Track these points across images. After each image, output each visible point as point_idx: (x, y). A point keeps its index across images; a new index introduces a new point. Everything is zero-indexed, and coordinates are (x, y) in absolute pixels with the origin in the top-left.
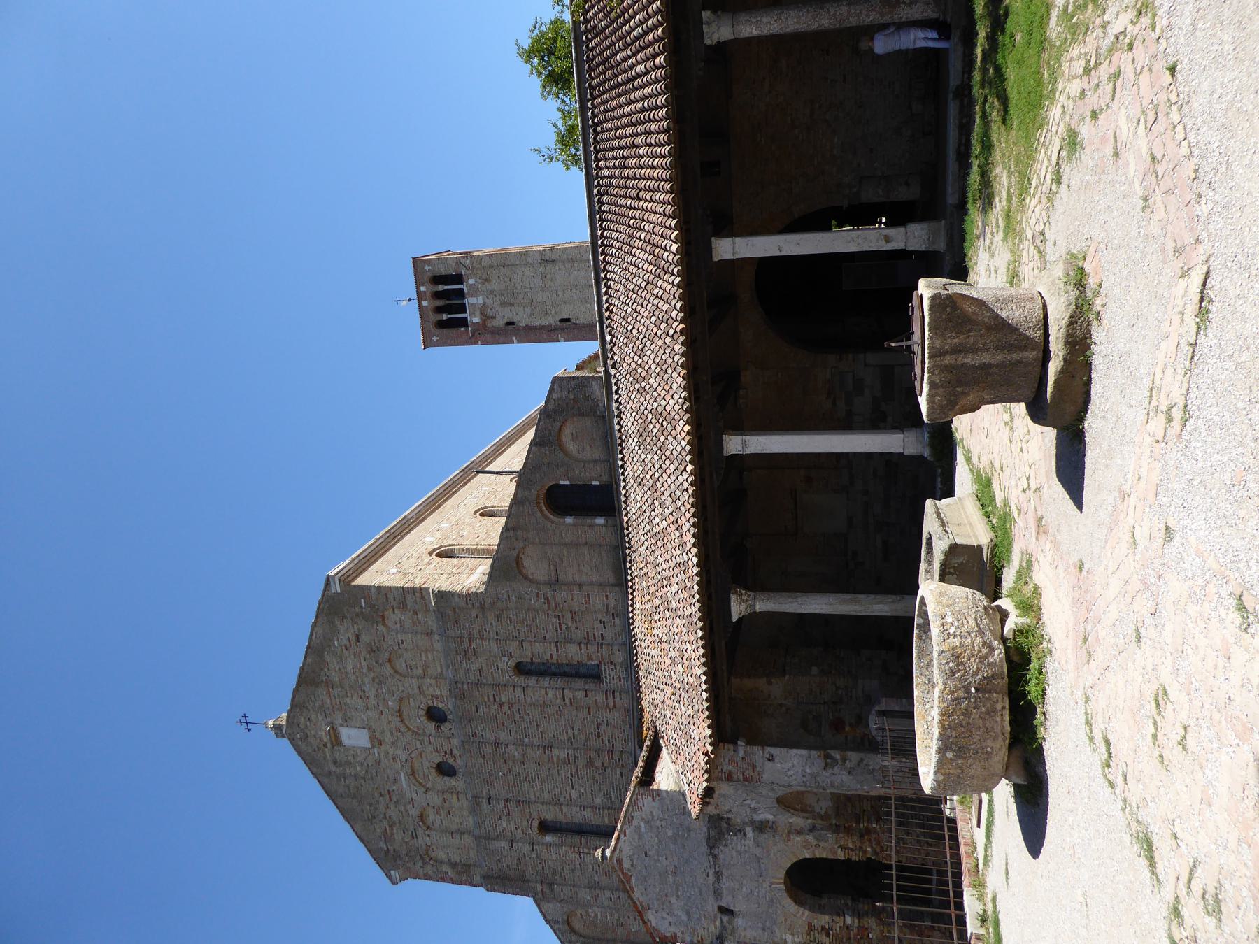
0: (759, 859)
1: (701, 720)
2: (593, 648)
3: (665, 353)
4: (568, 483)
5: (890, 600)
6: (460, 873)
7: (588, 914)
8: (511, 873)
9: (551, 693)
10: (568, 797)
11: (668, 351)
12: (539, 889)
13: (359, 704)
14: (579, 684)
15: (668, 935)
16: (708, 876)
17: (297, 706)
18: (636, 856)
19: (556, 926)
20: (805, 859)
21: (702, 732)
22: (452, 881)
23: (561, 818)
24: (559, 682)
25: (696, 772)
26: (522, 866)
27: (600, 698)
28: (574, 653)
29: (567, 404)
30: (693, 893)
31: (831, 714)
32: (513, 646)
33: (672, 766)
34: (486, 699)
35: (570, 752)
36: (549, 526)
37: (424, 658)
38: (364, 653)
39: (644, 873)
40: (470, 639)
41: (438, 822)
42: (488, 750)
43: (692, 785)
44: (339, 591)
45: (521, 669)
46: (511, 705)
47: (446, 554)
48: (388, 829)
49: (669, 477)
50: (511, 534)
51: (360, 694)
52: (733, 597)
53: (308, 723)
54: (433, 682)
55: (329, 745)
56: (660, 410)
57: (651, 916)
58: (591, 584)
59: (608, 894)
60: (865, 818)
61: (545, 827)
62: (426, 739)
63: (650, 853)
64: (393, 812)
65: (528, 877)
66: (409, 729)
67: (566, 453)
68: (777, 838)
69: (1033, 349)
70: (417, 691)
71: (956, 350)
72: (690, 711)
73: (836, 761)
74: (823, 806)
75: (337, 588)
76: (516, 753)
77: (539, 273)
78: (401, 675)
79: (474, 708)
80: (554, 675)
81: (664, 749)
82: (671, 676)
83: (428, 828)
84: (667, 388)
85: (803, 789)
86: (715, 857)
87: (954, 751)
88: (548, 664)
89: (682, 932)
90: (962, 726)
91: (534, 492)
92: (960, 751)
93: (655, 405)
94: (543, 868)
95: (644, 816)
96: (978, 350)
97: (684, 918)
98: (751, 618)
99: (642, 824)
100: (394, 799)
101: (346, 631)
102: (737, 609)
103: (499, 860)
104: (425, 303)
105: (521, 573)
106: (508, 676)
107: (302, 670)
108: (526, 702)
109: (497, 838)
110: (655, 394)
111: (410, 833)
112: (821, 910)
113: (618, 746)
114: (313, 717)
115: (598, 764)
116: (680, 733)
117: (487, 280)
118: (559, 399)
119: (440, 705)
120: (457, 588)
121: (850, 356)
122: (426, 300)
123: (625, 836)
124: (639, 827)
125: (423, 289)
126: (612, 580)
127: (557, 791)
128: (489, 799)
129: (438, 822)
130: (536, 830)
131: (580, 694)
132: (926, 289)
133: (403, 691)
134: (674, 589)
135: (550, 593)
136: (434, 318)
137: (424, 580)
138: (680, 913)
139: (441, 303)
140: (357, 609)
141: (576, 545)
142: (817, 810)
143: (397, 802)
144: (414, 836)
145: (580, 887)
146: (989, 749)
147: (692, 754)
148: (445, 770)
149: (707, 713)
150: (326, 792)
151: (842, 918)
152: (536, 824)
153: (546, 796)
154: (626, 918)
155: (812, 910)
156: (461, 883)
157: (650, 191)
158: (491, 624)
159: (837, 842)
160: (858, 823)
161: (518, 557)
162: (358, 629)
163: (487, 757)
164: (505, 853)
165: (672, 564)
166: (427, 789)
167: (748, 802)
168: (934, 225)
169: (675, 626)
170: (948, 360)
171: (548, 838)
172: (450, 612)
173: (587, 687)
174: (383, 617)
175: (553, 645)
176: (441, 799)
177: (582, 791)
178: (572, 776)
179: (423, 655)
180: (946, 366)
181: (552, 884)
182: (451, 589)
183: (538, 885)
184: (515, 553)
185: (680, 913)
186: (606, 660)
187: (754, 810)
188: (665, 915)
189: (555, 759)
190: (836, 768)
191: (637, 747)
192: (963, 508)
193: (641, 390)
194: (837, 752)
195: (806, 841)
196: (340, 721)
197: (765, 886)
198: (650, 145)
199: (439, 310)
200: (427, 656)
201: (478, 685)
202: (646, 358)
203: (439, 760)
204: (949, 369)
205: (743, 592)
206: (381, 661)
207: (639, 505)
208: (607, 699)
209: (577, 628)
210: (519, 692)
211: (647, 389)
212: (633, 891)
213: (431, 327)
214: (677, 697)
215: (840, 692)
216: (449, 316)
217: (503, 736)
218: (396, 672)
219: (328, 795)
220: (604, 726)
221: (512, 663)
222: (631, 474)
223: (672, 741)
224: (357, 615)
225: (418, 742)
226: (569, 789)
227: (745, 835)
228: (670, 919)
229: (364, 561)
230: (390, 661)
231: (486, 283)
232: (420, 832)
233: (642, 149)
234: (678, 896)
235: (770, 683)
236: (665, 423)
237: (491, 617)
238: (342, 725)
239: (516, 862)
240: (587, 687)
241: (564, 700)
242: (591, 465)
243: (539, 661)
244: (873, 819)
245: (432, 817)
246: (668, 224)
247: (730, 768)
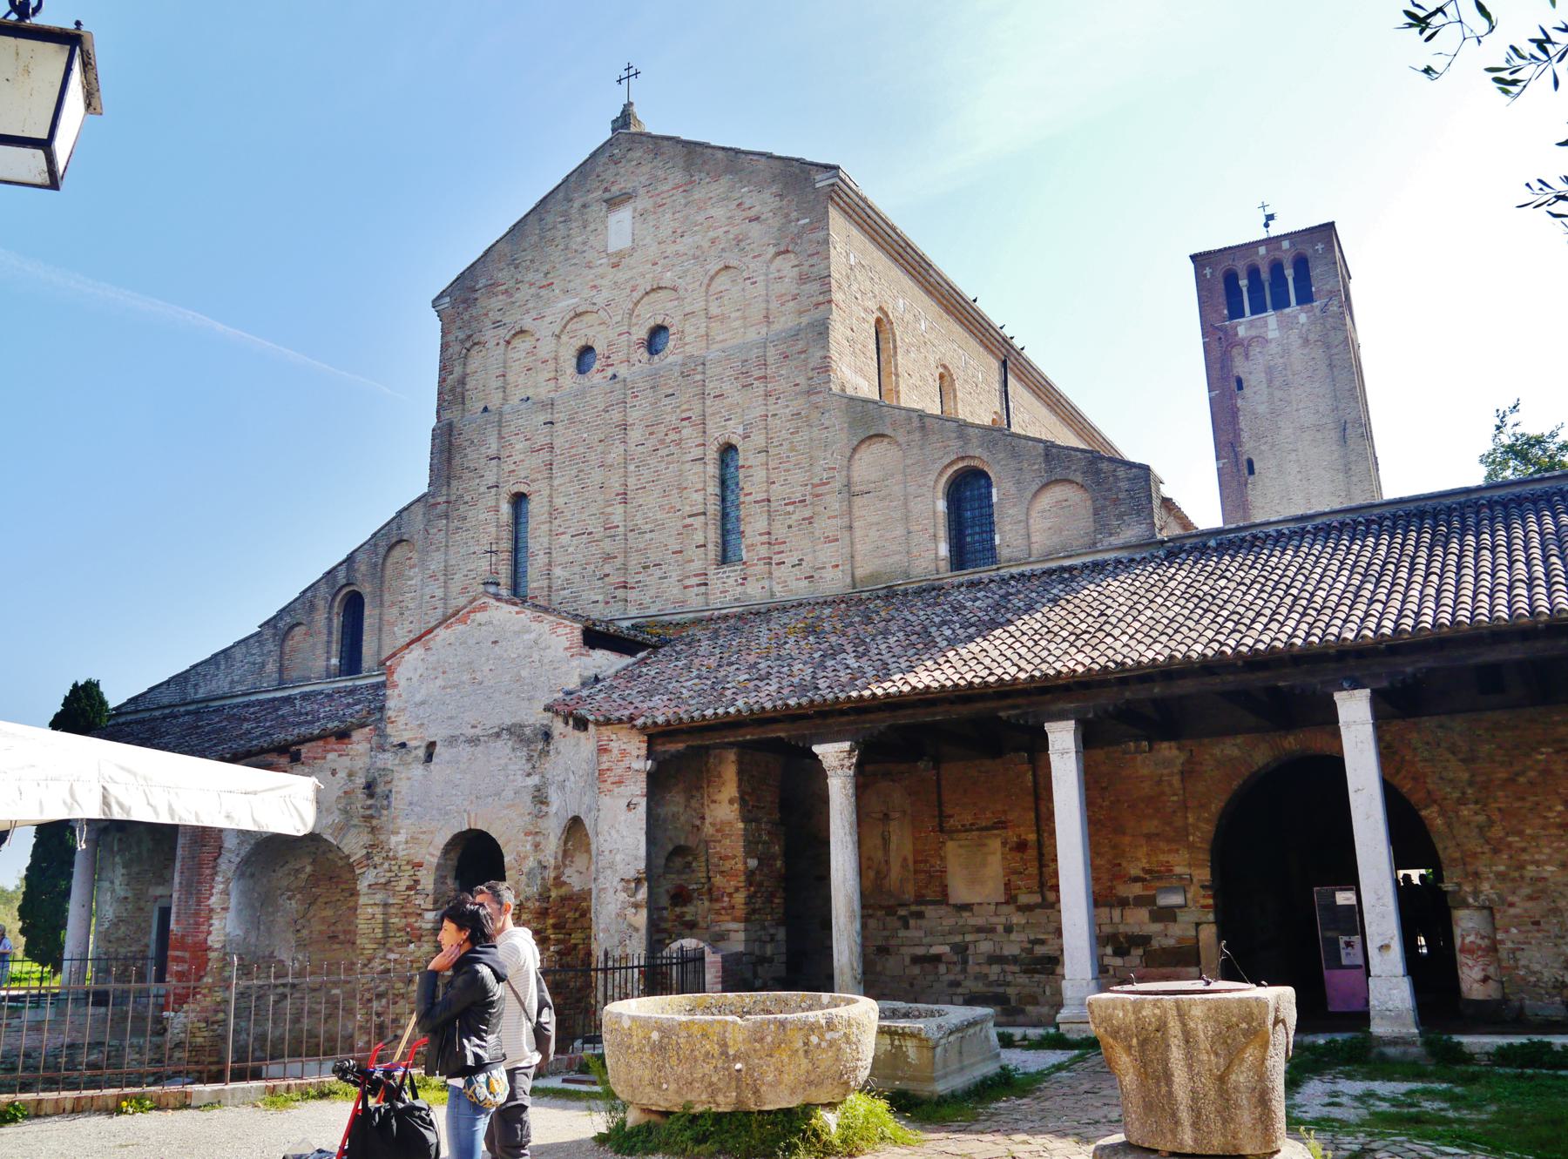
0: (498, 794)
1: (676, 709)
2: (763, 551)
3: (1190, 630)
4: (995, 499)
5: (855, 965)
6: (452, 390)
7: (414, 566)
8: (457, 461)
9: (698, 497)
10: (561, 530)
11: (1194, 635)
12: (440, 500)
13: (665, 232)
14: (713, 535)
16: (474, 727)
17: (658, 144)
18: (492, 629)
19: (394, 526)
20: (501, 856)
21: (661, 711)
22: (442, 381)
23: (532, 524)
24: (713, 508)
25: (606, 706)
26: (467, 475)
27: (697, 566)
28: (753, 525)
29: (1110, 490)
31: (695, 887)
32: (758, 439)
33: (612, 671)
34: (684, 407)
35: (621, 529)
36: (930, 477)
37: (733, 315)
38: (734, 231)
39: (471, 642)
40: (765, 377)
41: (516, 356)
42: (616, 416)
43: (589, 701)
44: (818, 185)
45: (728, 450)
46: (678, 443)
47: (882, 328)
49: (1010, 647)
50: (916, 423)
51: (679, 231)
52: (846, 745)
53: (634, 163)
54: (702, 331)
55: (607, 195)
56: (1107, 628)
57: (417, 651)
58: (852, 544)
59: (439, 593)
60: (561, 936)
61: (519, 500)
62: (625, 329)
64: (525, 292)
65: (454, 483)
66: (636, 304)
67: (1036, 495)
68: (527, 818)
69: (1196, 1140)
70: (688, 310)
71: (1188, 1038)
72: (686, 693)
73: (634, 895)
74: (574, 881)
75: (822, 181)
76: (616, 453)
77: (1324, 420)
78: (709, 285)
79: (670, 391)
80: (724, 500)
81: (634, 659)
82: (733, 664)
83: (508, 343)
84: (1139, 636)
85: (594, 853)
86: (498, 735)
87: (660, 1042)
88: (737, 491)
89: (400, 696)
90: (692, 1051)
91: (977, 452)
92: (660, 1048)
93: (1114, 620)
96: (1190, 1067)
97: (418, 698)
98: (816, 772)
99: (533, 636)
100: (543, 292)
101: (764, 201)
102: (833, 754)
104: (1262, 250)
105: (862, 441)
106: (716, 435)
108: (683, 463)
109: (501, 437)
110: (1129, 619)
112: (440, 880)
113: (632, 595)
114: (644, 169)
115: (607, 569)
116: (656, 681)
117: (1306, 341)
118: (1117, 479)
119: (671, 344)
120: (834, 354)
121: (1211, 901)
122: (1268, 251)
123: (517, 613)
124: (529, 631)
125: (1286, 244)
126: (859, 573)
127: (568, 514)
128: (552, 423)
129: (516, 356)
130: (515, 489)
131: (699, 538)
132: (1281, 998)
133: (686, 290)
134: (852, 662)
135: (837, 485)
136: (1241, 268)
137: (842, 305)
138: (423, 691)
139: (1265, 275)
140: (794, 215)
141: (906, 519)
142: (568, 871)
143: (538, 296)
144: (497, 324)
145: (446, 554)
146: (665, 1086)
147: (629, 699)
148: (585, 353)
149: (685, 717)
150: (545, 198)
151: (431, 907)
152: (523, 489)
153: (559, 501)
154: (411, 619)
155: (439, 867)
156: (440, 393)
157: (1439, 591)
158: (787, 406)
159: (527, 899)
160: (555, 926)
161: (883, 436)
162: (767, 219)
163: (607, 415)
164: (483, 450)
165: (886, 657)
166: (558, 337)
167: (572, 778)
168: (1410, 1017)
169: (801, 666)
170: (1174, 1027)
171: (505, 508)
172: (801, 345)
173: (711, 546)
174: (787, 251)
175: (764, 496)
176: (547, 357)
179: (739, 314)
180: (1165, 1024)
181: (447, 517)
182: (833, 345)
183: (444, 498)
184: (888, 432)
185: (423, 691)
186: (750, 571)
187: (562, 787)
188: (419, 672)
189: (609, 510)
190: (625, 895)
191: (633, 621)
192: (984, 1060)
193: (1135, 598)
194: (646, 896)
195: (525, 858)
196: (639, 208)
197: (465, 803)
198: (1511, 588)
199: (1254, 273)
200: (737, 319)
201: (703, 395)
202: (1182, 602)
203: (598, 349)
204: (1162, 1027)
205: (854, 760)
206: (724, 255)
207: (969, 604)
208: (696, 575)
209: (790, 527)
210: (698, 452)
211: (1138, 606)
212: (447, 627)
213: (1226, 264)
214: (704, 674)
215: (726, 899)
216: (1245, 290)
217: (635, 435)
218: (712, 278)
219: (541, 201)
220: (658, 573)
221: (735, 440)
222: (1012, 590)
223: (644, 670)
224: (787, 215)
225: (619, 318)
226: (572, 531)
227: (529, 775)
229: (863, 215)
230: (727, 267)
231: (1300, 341)
232: (502, 332)
233: (1506, 575)
234: (444, 688)
235: (731, 802)
236: (1086, 636)
237: (795, 406)
238: (635, 210)
239: (472, 465)
240: (711, 546)
241: (690, 516)
242: (1023, 532)
243: (741, 476)
244: (561, 946)
245: (522, 345)
246: (1385, 623)
247: (615, 751)
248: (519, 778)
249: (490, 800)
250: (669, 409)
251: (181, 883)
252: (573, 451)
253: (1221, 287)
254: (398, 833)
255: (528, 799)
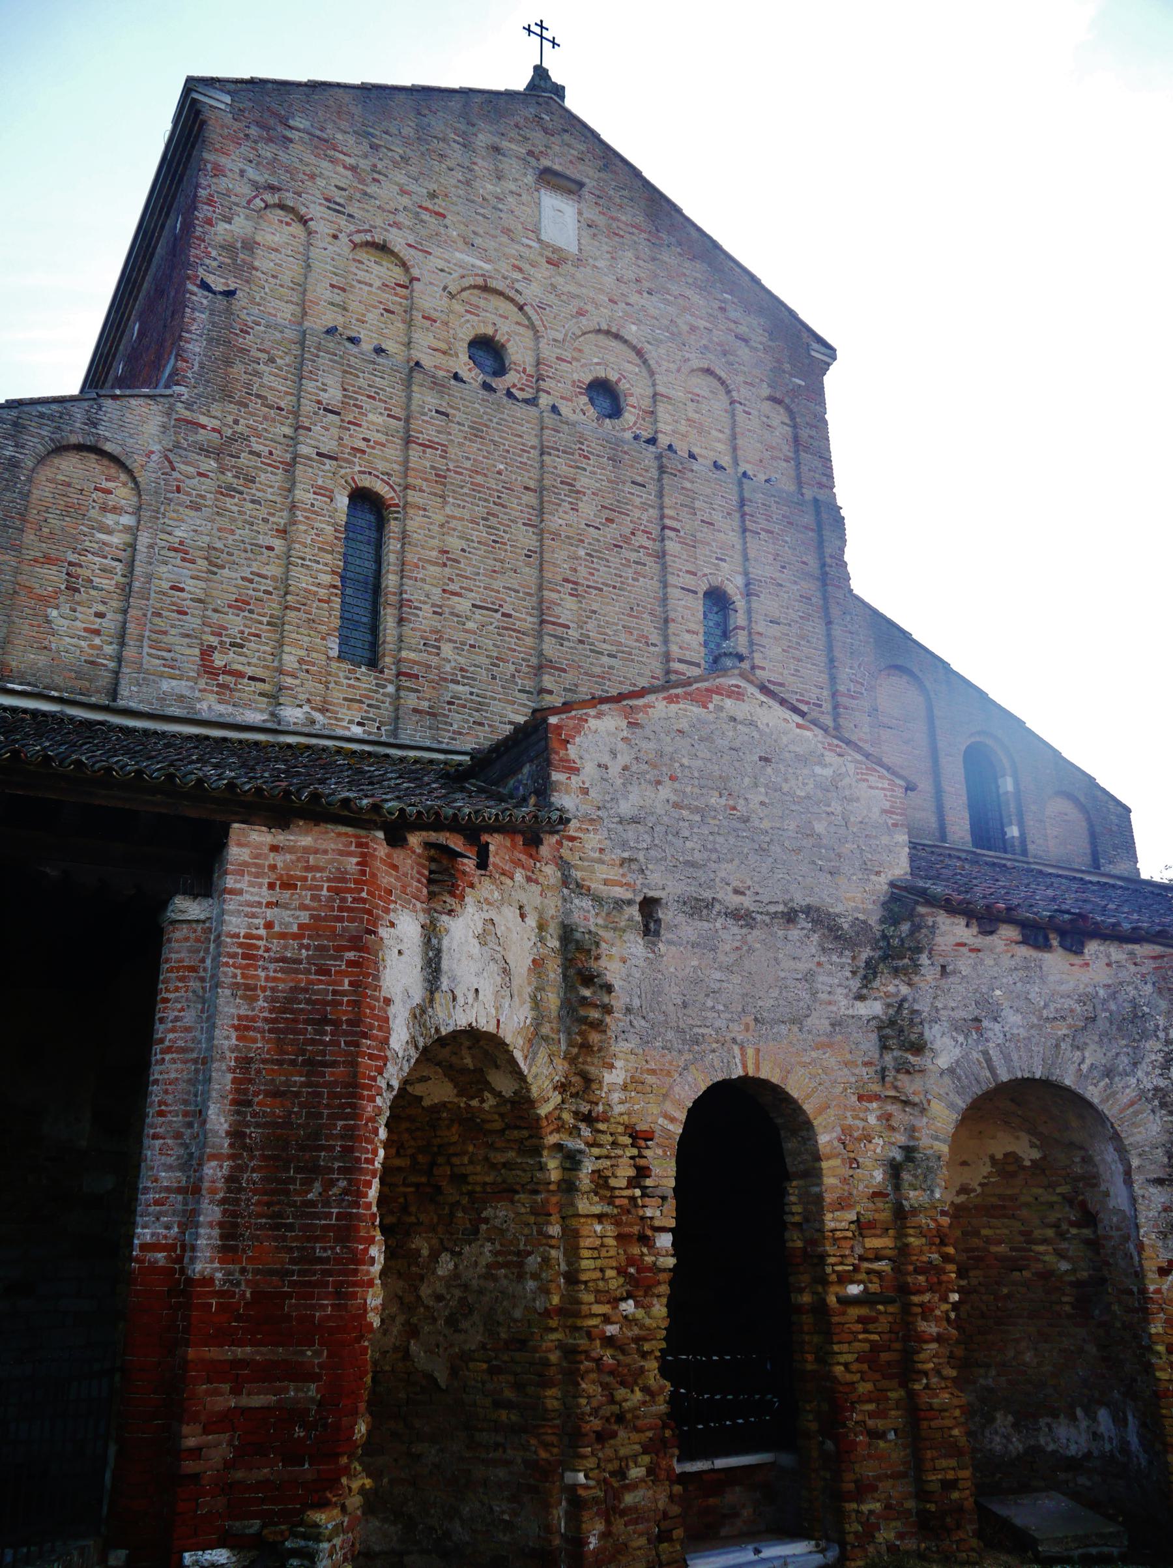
0: (798, 1021)
7: (116, 510)
12: (203, 420)
15: (572, 751)
16: (737, 892)
18: (755, 734)
30: (689, 844)
48: (348, 160)
63: (769, 770)
86: (790, 917)
89: (585, 791)
94: (259, 455)
95: (847, 781)
97: (626, 808)
99: (828, 772)
103: (272, 360)
107: (678, 210)
111: (342, 201)
130: (366, 482)
154: (102, 608)
177: (470, 625)
178: (504, 615)
197: (734, 1027)
212: (671, 700)
227: (860, 998)
228: (615, 769)
234: (676, 805)
241: (680, 661)
248: (844, 1002)
249: (783, 1028)
250: (638, 501)
251: (236, 1135)
252: (479, 479)
254: (612, 1066)
255: (869, 1043)
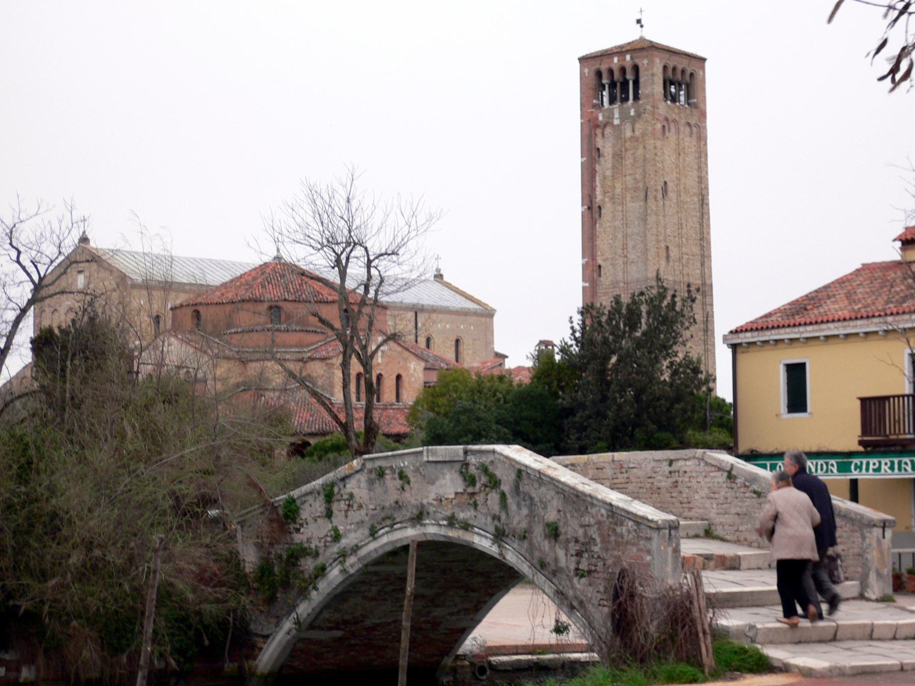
104: (616, 60)
122: (618, 61)
136: (604, 68)
199: (611, 72)
253: (592, 81)
